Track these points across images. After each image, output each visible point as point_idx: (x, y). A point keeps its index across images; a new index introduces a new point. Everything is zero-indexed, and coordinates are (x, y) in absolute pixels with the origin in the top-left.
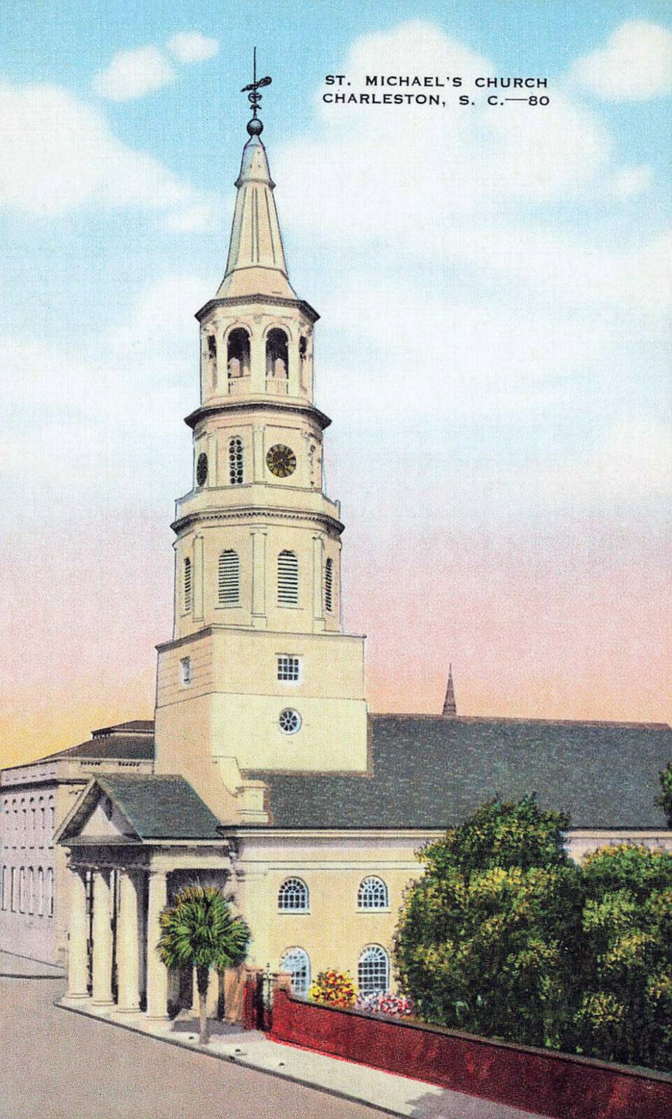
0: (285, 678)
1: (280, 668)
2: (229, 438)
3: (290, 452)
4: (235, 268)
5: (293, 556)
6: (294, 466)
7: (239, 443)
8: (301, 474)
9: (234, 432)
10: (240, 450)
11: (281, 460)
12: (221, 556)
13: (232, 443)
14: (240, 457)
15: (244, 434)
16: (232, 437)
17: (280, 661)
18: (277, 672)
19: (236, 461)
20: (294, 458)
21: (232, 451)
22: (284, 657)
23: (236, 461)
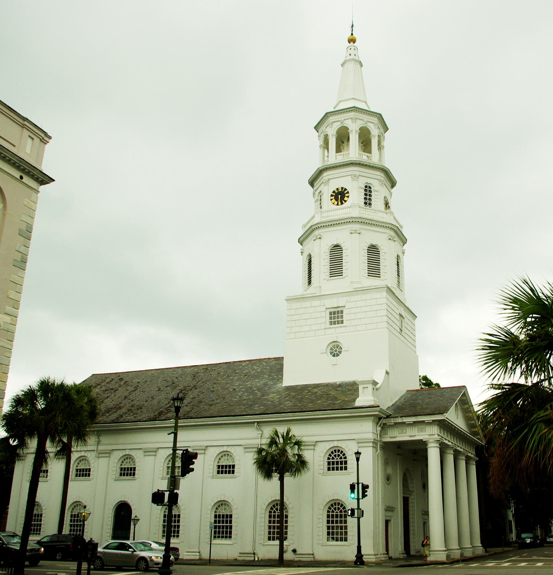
12: (331, 250)
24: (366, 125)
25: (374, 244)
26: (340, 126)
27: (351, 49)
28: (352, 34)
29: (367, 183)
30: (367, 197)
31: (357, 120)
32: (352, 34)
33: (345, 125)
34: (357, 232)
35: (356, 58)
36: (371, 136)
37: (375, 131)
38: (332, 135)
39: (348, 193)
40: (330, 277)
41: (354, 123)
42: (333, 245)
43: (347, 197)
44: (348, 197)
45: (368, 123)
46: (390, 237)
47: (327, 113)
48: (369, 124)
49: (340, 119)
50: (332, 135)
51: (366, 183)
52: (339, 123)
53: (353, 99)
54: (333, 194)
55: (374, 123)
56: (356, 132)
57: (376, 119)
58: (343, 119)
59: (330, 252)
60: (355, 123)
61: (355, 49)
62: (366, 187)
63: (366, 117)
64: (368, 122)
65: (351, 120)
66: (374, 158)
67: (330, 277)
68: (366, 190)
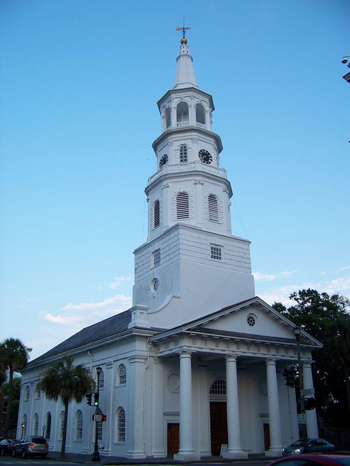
0: (215, 258)
1: (212, 252)
2: (180, 145)
3: (209, 154)
4: (179, 83)
5: (215, 198)
6: (211, 160)
7: (185, 147)
8: (213, 163)
9: (183, 142)
10: (185, 150)
11: (205, 157)
12: (178, 196)
13: (181, 148)
14: (186, 153)
15: (189, 143)
16: (181, 144)
17: (212, 248)
18: (211, 254)
19: (183, 155)
20: (211, 157)
21: (181, 151)
22: (214, 246)
23: (183, 155)
24: (201, 103)
25: (214, 193)
26: (180, 102)
27: (184, 47)
28: (184, 38)
31: (195, 98)
32: (184, 38)
34: (200, 182)
37: (207, 108)
40: (177, 219)
41: (192, 100)
42: (180, 192)
45: (202, 101)
46: (224, 189)
48: (202, 102)
49: (180, 96)
50: (174, 108)
55: (206, 102)
56: (194, 107)
57: (208, 100)
58: (183, 97)
59: (177, 198)
60: (193, 100)
61: (187, 48)
63: (201, 97)
64: (203, 100)
65: (189, 98)
66: (207, 127)
67: (177, 219)
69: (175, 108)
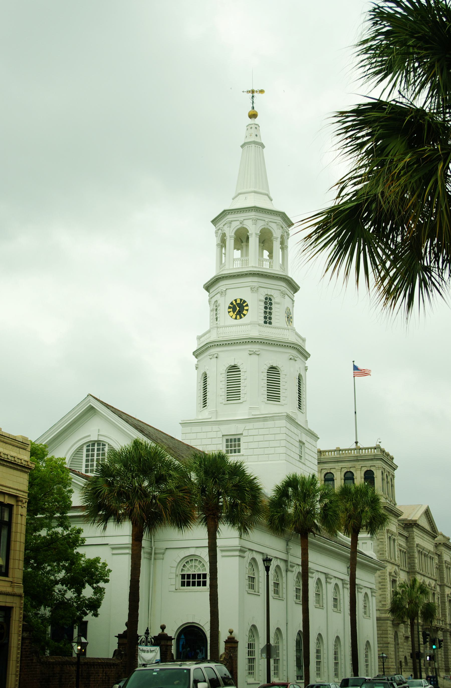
28: (253, 108)
29: (267, 294)
30: (267, 310)
32: (253, 108)
33: (244, 226)
35: (257, 140)
36: (272, 238)
38: (231, 237)
39: (247, 305)
43: (245, 310)
44: (247, 310)
47: (224, 211)
51: (266, 295)
52: (238, 223)
53: (255, 192)
54: (231, 306)
61: (256, 128)
62: (266, 299)
68: (266, 303)
69: (232, 237)
